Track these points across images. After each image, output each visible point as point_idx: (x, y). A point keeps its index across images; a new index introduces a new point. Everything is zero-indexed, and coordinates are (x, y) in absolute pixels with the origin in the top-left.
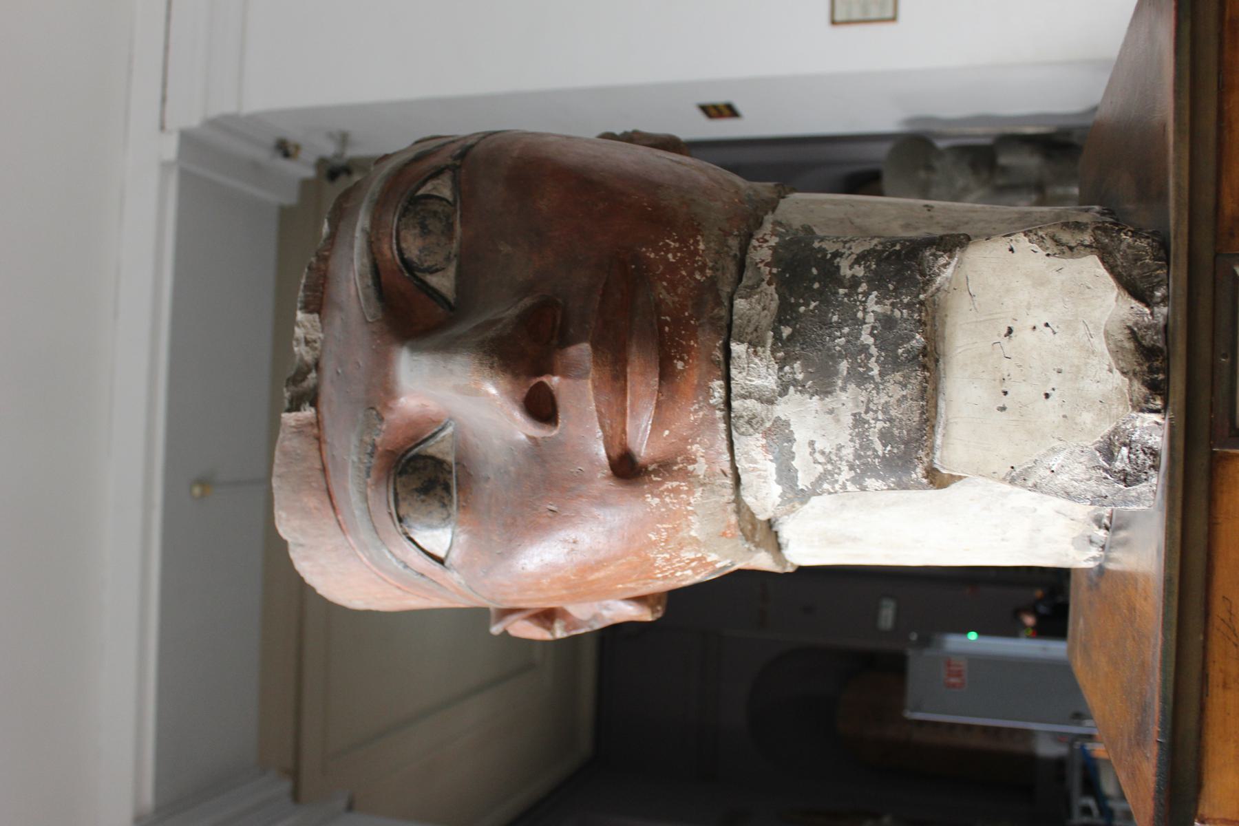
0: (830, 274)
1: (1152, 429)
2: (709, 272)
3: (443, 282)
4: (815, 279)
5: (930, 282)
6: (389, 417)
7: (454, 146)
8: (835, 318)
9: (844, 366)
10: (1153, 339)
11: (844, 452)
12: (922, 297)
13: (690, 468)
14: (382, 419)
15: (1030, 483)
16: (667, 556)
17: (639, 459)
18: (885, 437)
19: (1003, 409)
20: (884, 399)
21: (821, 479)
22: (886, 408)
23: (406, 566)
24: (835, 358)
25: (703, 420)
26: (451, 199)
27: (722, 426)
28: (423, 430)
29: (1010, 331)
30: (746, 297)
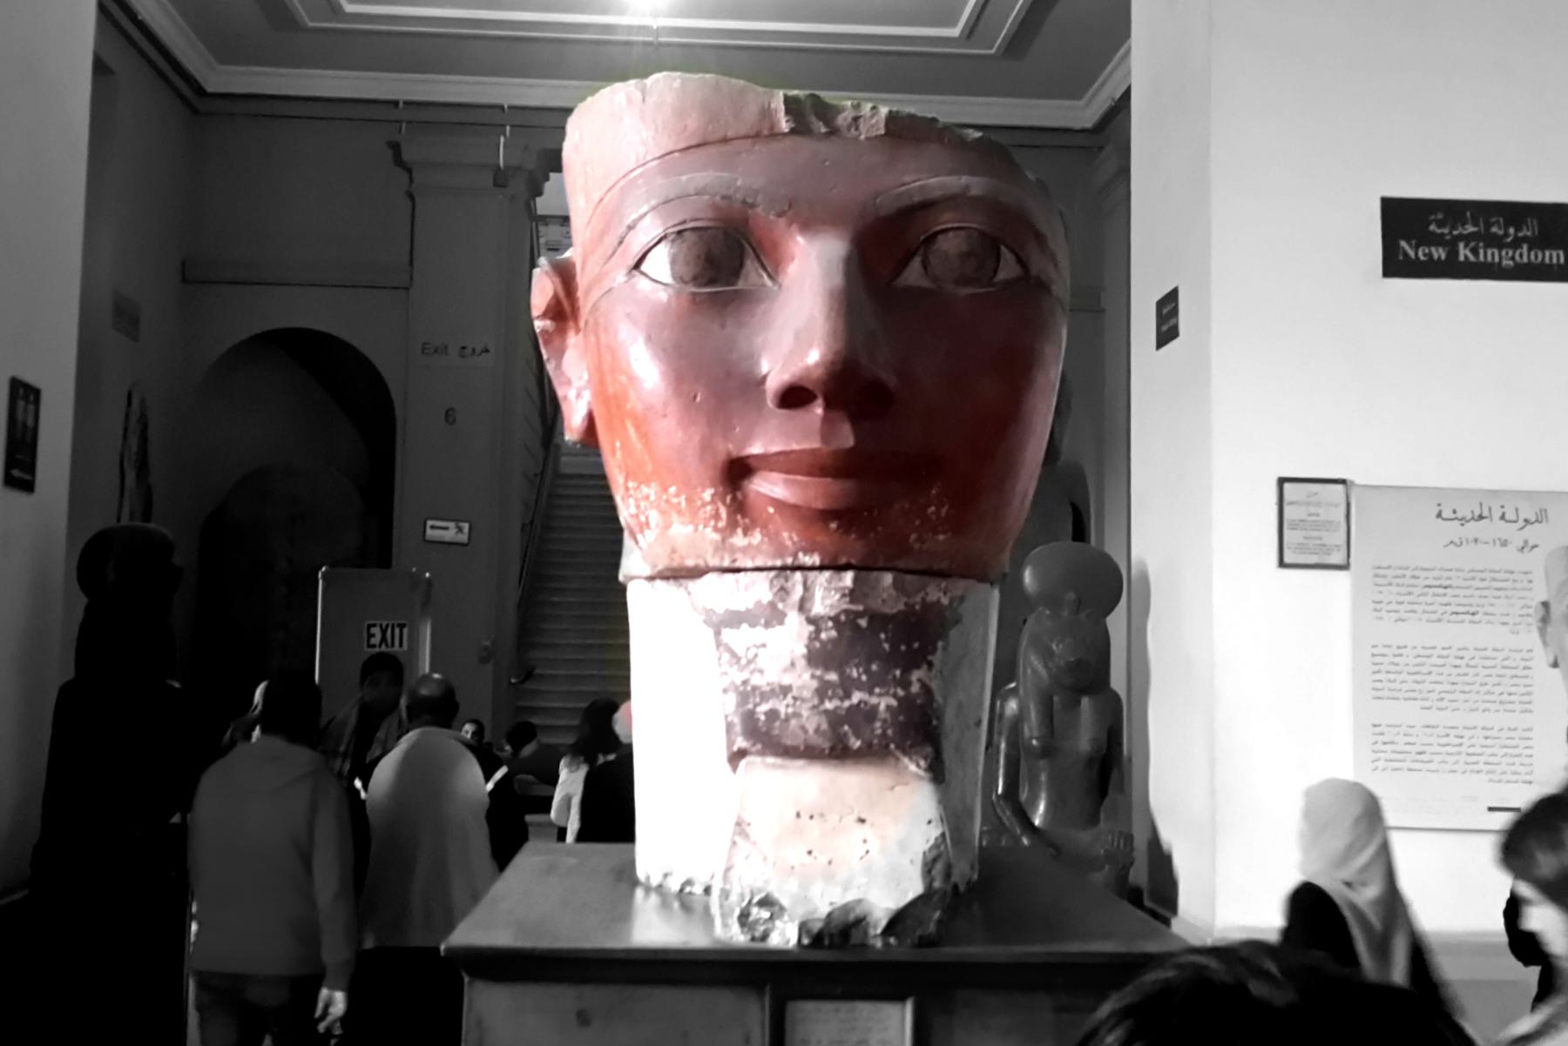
0: (912, 661)
1: (785, 936)
2: (917, 546)
3: (913, 275)
4: (909, 645)
5: (905, 752)
6: (782, 221)
7: (1051, 269)
8: (874, 667)
9: (833, 677)
10: (855, 938)
11: (757, 675)
12: (892, 746)
13: (739, 531)
14: (779, 215)
15: (737, 839)
16: (652, 498)
17: (746, 483)
18: (772, 714)
19: (798, 815)
20: (805, 713)
21: (734, 654)
22: (797, 715)
23: (630, 228)
24: (840, 668)
25: (786, 547)
26: (996, 280)
27: (779, 563)
28: (771, 260)
29: (862, 821)
30: (895, 584)
